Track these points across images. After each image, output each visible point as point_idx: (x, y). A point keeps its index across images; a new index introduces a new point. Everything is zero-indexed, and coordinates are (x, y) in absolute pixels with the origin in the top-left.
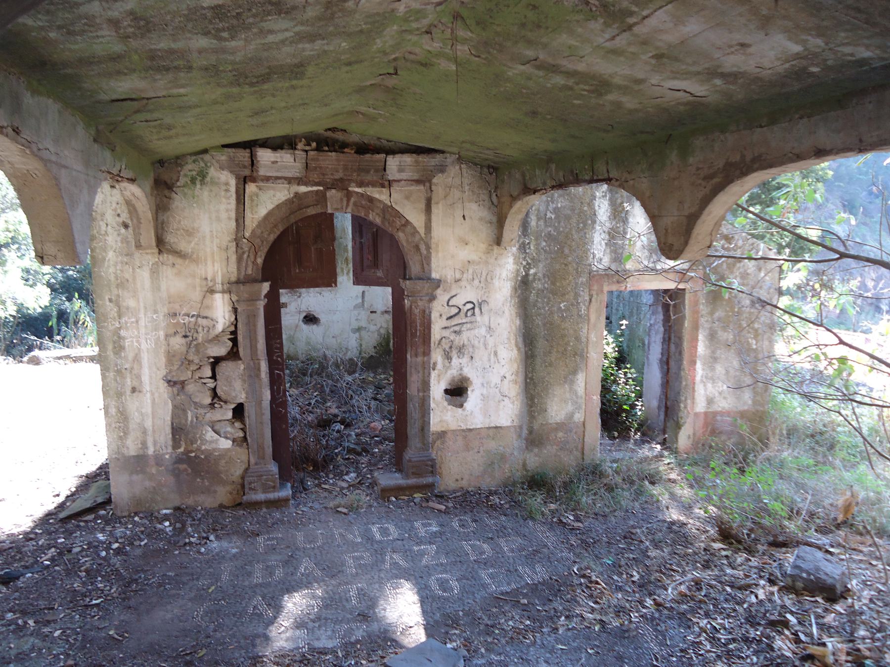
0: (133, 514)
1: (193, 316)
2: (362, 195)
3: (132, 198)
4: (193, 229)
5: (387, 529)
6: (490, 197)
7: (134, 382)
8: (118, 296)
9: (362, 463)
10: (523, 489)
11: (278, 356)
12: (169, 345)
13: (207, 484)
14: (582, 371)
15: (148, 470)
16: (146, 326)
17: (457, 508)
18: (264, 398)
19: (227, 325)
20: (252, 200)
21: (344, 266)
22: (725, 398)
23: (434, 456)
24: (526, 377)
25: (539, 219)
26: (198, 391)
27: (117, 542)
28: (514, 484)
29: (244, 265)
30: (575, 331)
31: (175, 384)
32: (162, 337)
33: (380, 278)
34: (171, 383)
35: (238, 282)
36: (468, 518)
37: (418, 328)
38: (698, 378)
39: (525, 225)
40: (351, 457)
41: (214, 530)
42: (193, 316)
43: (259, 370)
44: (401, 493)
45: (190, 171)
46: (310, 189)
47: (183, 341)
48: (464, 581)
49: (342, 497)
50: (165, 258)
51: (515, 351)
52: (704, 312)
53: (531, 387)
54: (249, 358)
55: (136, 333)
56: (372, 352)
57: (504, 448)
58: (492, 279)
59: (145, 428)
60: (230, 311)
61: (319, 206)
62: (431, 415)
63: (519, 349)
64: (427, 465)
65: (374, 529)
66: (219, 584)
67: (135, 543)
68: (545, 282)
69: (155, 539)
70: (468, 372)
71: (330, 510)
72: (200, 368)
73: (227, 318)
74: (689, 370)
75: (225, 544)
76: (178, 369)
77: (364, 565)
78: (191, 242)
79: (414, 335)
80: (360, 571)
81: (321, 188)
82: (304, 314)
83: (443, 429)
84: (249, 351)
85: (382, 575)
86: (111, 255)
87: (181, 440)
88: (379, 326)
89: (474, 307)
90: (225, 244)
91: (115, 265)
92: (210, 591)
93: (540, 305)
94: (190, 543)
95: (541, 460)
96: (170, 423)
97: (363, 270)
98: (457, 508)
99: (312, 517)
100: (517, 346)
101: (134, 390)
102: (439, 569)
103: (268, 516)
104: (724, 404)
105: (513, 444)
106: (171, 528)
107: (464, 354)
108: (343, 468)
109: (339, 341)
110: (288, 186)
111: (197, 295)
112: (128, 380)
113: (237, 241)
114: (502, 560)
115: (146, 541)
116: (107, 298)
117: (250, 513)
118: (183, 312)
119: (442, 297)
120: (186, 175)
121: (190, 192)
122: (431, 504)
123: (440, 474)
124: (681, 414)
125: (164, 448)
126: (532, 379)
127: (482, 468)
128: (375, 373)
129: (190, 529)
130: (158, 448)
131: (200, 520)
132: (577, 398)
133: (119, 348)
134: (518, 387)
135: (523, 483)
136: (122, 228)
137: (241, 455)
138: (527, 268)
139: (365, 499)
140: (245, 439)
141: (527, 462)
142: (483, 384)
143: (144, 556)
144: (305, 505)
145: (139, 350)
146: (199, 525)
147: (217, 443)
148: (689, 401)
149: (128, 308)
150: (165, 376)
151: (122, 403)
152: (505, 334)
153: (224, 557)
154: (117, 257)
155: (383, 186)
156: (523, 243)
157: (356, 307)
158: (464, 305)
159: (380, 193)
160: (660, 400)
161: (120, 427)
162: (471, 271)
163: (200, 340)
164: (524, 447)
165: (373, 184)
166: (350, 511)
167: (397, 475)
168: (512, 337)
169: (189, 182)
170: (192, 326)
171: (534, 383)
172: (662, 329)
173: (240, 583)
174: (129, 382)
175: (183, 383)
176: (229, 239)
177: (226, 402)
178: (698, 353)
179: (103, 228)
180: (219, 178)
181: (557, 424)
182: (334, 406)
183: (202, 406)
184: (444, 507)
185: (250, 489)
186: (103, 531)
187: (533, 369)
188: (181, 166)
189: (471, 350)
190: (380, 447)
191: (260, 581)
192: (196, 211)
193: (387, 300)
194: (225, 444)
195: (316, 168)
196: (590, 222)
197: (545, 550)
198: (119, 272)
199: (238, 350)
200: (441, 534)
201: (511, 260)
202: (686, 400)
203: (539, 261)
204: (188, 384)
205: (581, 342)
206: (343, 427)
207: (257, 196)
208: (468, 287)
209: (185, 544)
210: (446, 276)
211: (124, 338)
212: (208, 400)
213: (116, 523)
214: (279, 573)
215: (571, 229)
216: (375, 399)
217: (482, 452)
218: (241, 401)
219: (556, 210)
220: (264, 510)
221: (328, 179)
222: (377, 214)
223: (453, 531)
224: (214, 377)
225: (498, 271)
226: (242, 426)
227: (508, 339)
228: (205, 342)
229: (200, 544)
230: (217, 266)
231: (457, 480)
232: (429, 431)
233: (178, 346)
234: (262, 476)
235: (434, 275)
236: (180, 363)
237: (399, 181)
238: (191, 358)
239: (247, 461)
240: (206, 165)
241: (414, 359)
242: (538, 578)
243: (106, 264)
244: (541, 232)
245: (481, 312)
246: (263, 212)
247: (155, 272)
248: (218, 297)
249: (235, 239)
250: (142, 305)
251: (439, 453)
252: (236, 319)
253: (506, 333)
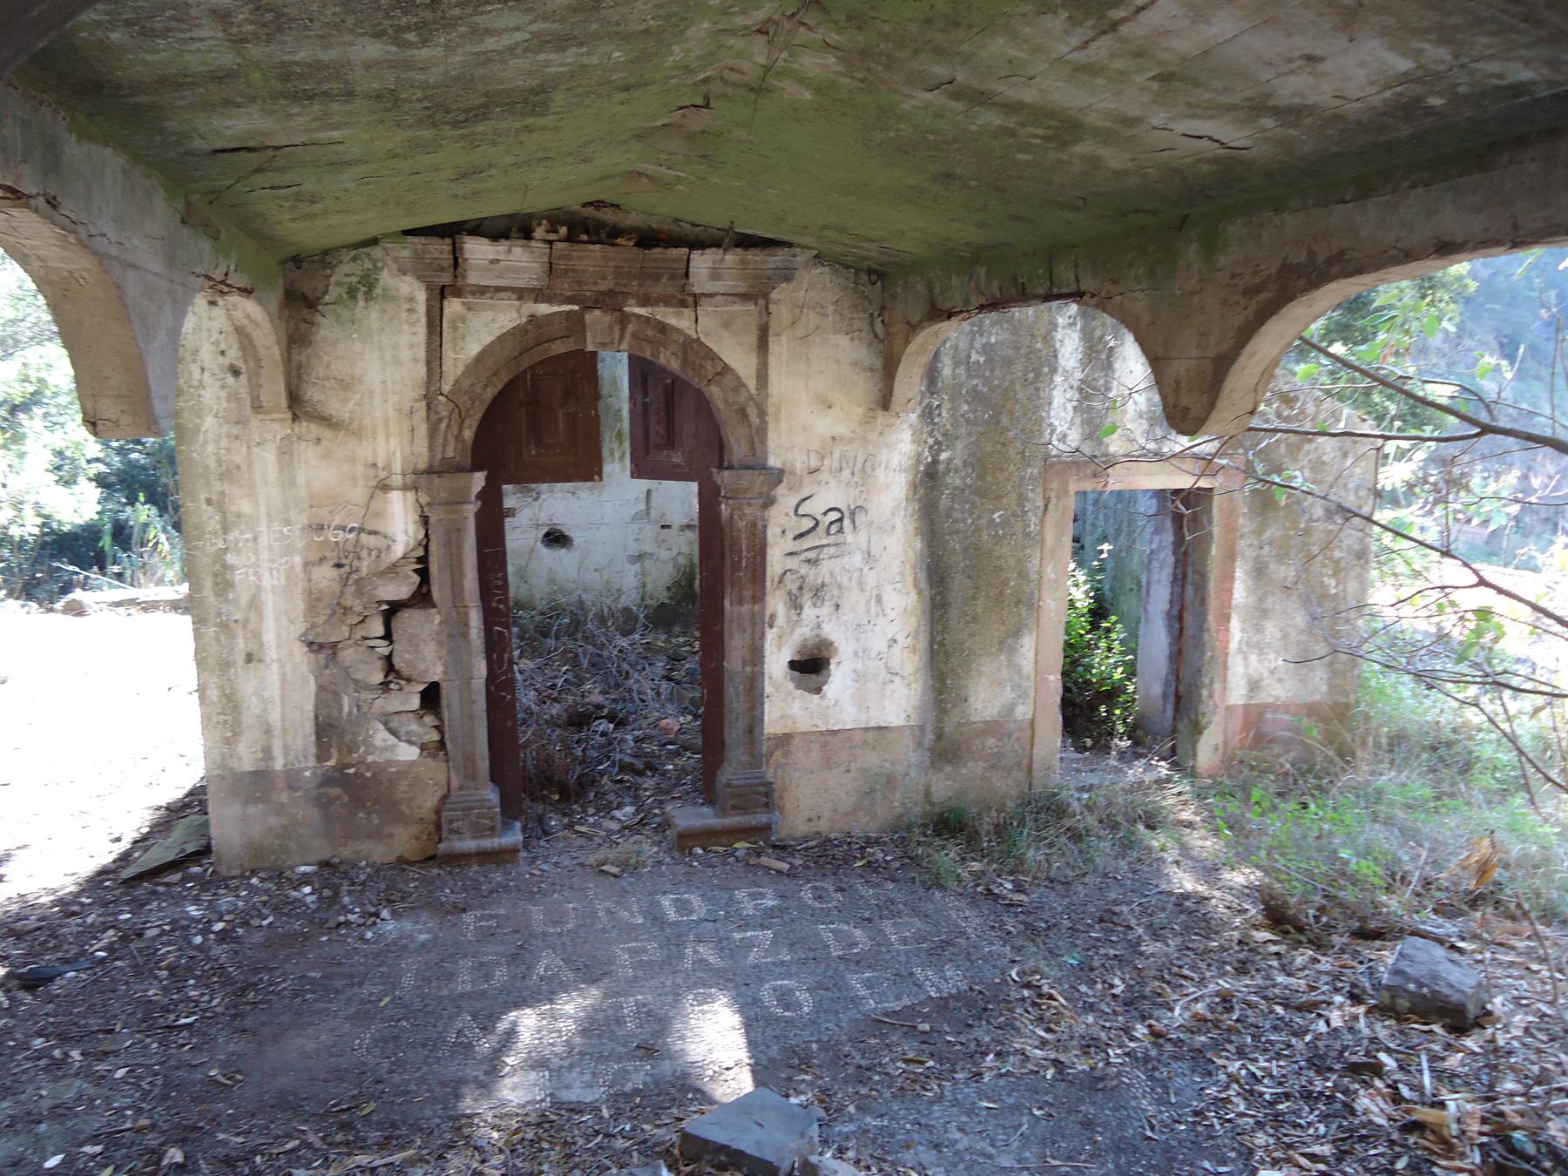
0: (247, 874)
1: (351, 530)
2: (648, 319)
3: (245, 322)
4: (352, 377)
5: (688, 901)
6: (872, 324)
7: (250, 646)
8: (222, 493)
9: (646, 789)
10: (925, 835)
11: (499, 601)
12: (310, 581)
13: (376, 821)
14: (1031, 631)
15: (275, 797)
16: (270, 548)
17: (809, 868)
18: (475, 673)
19: (411, 546)
20: (455, 328)
21: (615, 446)
22: (1280, 680)
23: (769, 776)
24: (932, 641)
25: (956, 364)
26: (362, 661)
27: (220, 920)
28: (909, 828)
29: (441, 441)
30: (1019, 561)
32: (298, 565)
33: (678, 466)
34: (314, 646)
35: (430, 471)
36: (828, 885)
37: (744, 554)
38: (1233, 645)
39: (932, 374)
40: (626, 778)
41: (389, 901)
42: (351, 530)
43: (466, 624)
44: (713, 840)
45: (346, 275)
46: (556, 309)
47: (335, 573)
48: (821, 992)
49: (611, 847)
50: (304, 429)
51: (914, 596)
52: (1245, 530)
53: (941, 657)
54: (449, 604)
55: (253, 559)
56: (663, 597)
57: (892, 764)
58: (874, 469)
59: (268, 724)
60: (415, 522)
61: (571, 340)
62: (766, 706)
63: (920, 592)
64: (758, 794)
65: (666, 902)
66: (397, 993)
67: (252, 922)
68: (967, 476)
69: (286, 915)
70: (831, 631)
71: (589, 870)
72: (362, 621)
73: (411, 533)
74: (1218, 631)
75: (407, 926)
76: (326, 621)
77: (649, 963)
78: (346, 401)
79: (736, 567)
80: (640, 973)
81: (576, 308)
83: (787, 731)
84: (448, 593)
85: (679, 980)
86: (209, 422)
87: (331, 746)
88: (675, 551)
89: (841, 519)
90: (407, 404)
91: (218, 440)
92: (382, 1004)
93: (957, 515)
94: (347, 924)
95: (957, 786)
96: (312, 715)
97: (648, 453)
98: (809, 868)
99: (557, 881)
100: (916, 586)
101: (250, 658)
102: (778, 970)
103: (482, 879)
104: (1278, 691)
105: (908, 758)
106: (314, 898)
107: (823, 600)
108: (611, 797)
109: (605, 577)
110: (516, 303)
111: (358, 494)
112: (240, 640)
113: (429, 398)
114: (888, 957)
115: (271, 919)
116: (203, 496)
117: (450, 873)
118: (335, 523)
119: (786, 500)
120: (339, 284)
121: (346, 313)
122: (764, 860)
123: (781, 809)
124: (1202, 708)
125: (301, 759)
126: (942, 644)
127: (853, 799)
128: (669, 633)
129: (346, 900)
130: (290, 758)
131: (363, 883)
132: (1021, 678)
133: (224, 585)
134: (917, 658)
135: (925, 826)
136: (229, 375)
137: (435, 772)
138: (936, 449)
139: (649, 850)
140: (441, 744)
141: (933, 789)
142: (856, 653)
143: (267, 944)
144: (546, 860)
145: (259, 588)
146: (362, 892)
147: (393, 751)
148: (1217, 686)
149: (239, 516)
150: (304, 635)
152: (896, 567)
153: (405, 947)
154: (221, 426)
155: (684, 304)
156: (929, 406)
157: (635, 518)
158: (825, 514)
159: (679, 315)
160: (1167, 684)
161: (226, 721)
162: (836, 455)
163: (364, 571)
164: (928, 762)
165: (666, 301)
166: (623, 871)
167: (705, 809)
168: (909, 572)
169: (345, 296)
170: (349, 547)
171: (946, 652)
172: (1171, 559)
173: (434, 991)
174: (241, 645)
175: (334, 645)
176: (414, 395)
177: (409, 680)
178: (1234, 602)
179: (196, 375)
180: (397, 290)
181: (985, 722)
182: (597, 690)
183: (368, 688)
184: (788, 866)
185: (451, 831)
186: (196, 901)
187: (945, 628)
188: (331, 266)
189: (835, 592)
190: (677, 761)
191: (469, 987)
192: (357, 346)
193: (690, 506)
194: (408, 753)
195: (566, 272)
196: (1046, 370)
197: (962, 941)
198: (223, 451)
199: (429, 591)
200: (782, 910)
201: (907, 436)
202: (1211, 683)
203: (957, 438)
204: (343, 649)
205: (1029, 581)
206: (612, 726)
207: (464, 320)
208: (832, 483)
209: (339, 925)
210: (793, 465)
211: (232, 568)
212: (378, 677)
213: (219, 888)
214: (501, 975)
215: (1013, 382)
216: (669, 679)
217: (853, 773)
218: (436, 679)
219: (987, 349)
220: (476, 868)
221: (588, 290)
222: (673, 354)
223: (803, 907)
224: (388, 636)
225: (884, 455)
226: (437, 722)
227: (902, 574)
228: (374, 575)
229: (364, 924)
230: (394, 442)
231: (810, 820)
232: (762, 733)
233: (325, 583)
234: (471, 809)
235: (773, 462)
236: (329, 612)
237: (711, 295)
238: (348, 603)
239: (444, 783)
240: (375, 266)
241: (736, 608)
242: (949, 988)
243: (201, 437)
244: (961, 386)
245: (855, 527)
246: (473, 348)
247: (285, 453)
248: (395, 496)
249: (426, 396)
250: (263, 510)
251: (780, 772)
252: (427, 535)
253: (898, 563)
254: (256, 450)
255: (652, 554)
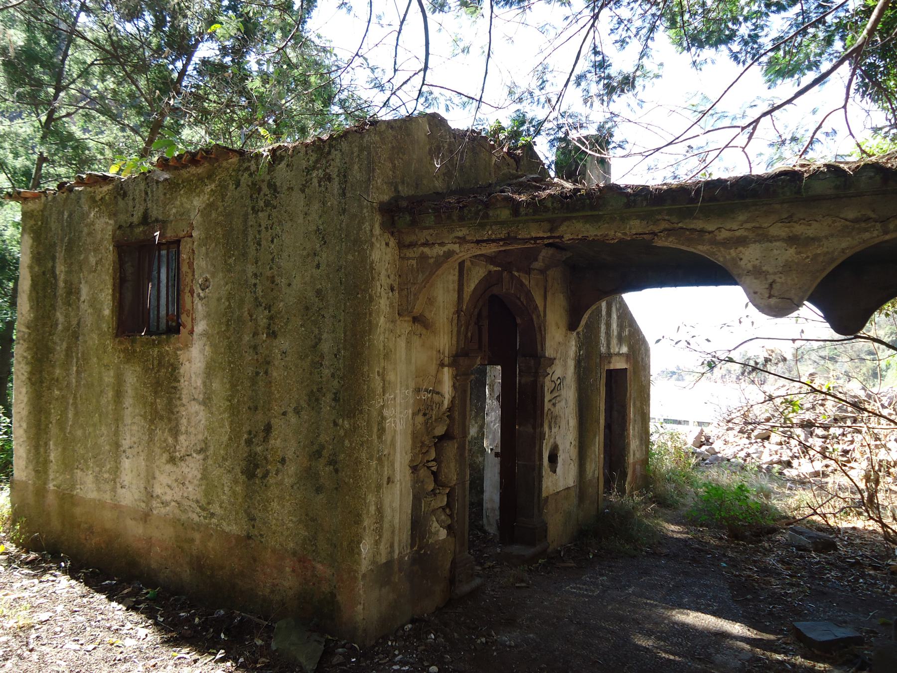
0: (381, 641)
31: (414, 469)
32: (410, 416)
86: (382, 319)
112: (386, 469)
113: (458, 312)
145: (395, 431)
151: (380, 498)
246: (473, 286)
248: (446, 369)
254: (398, 339)
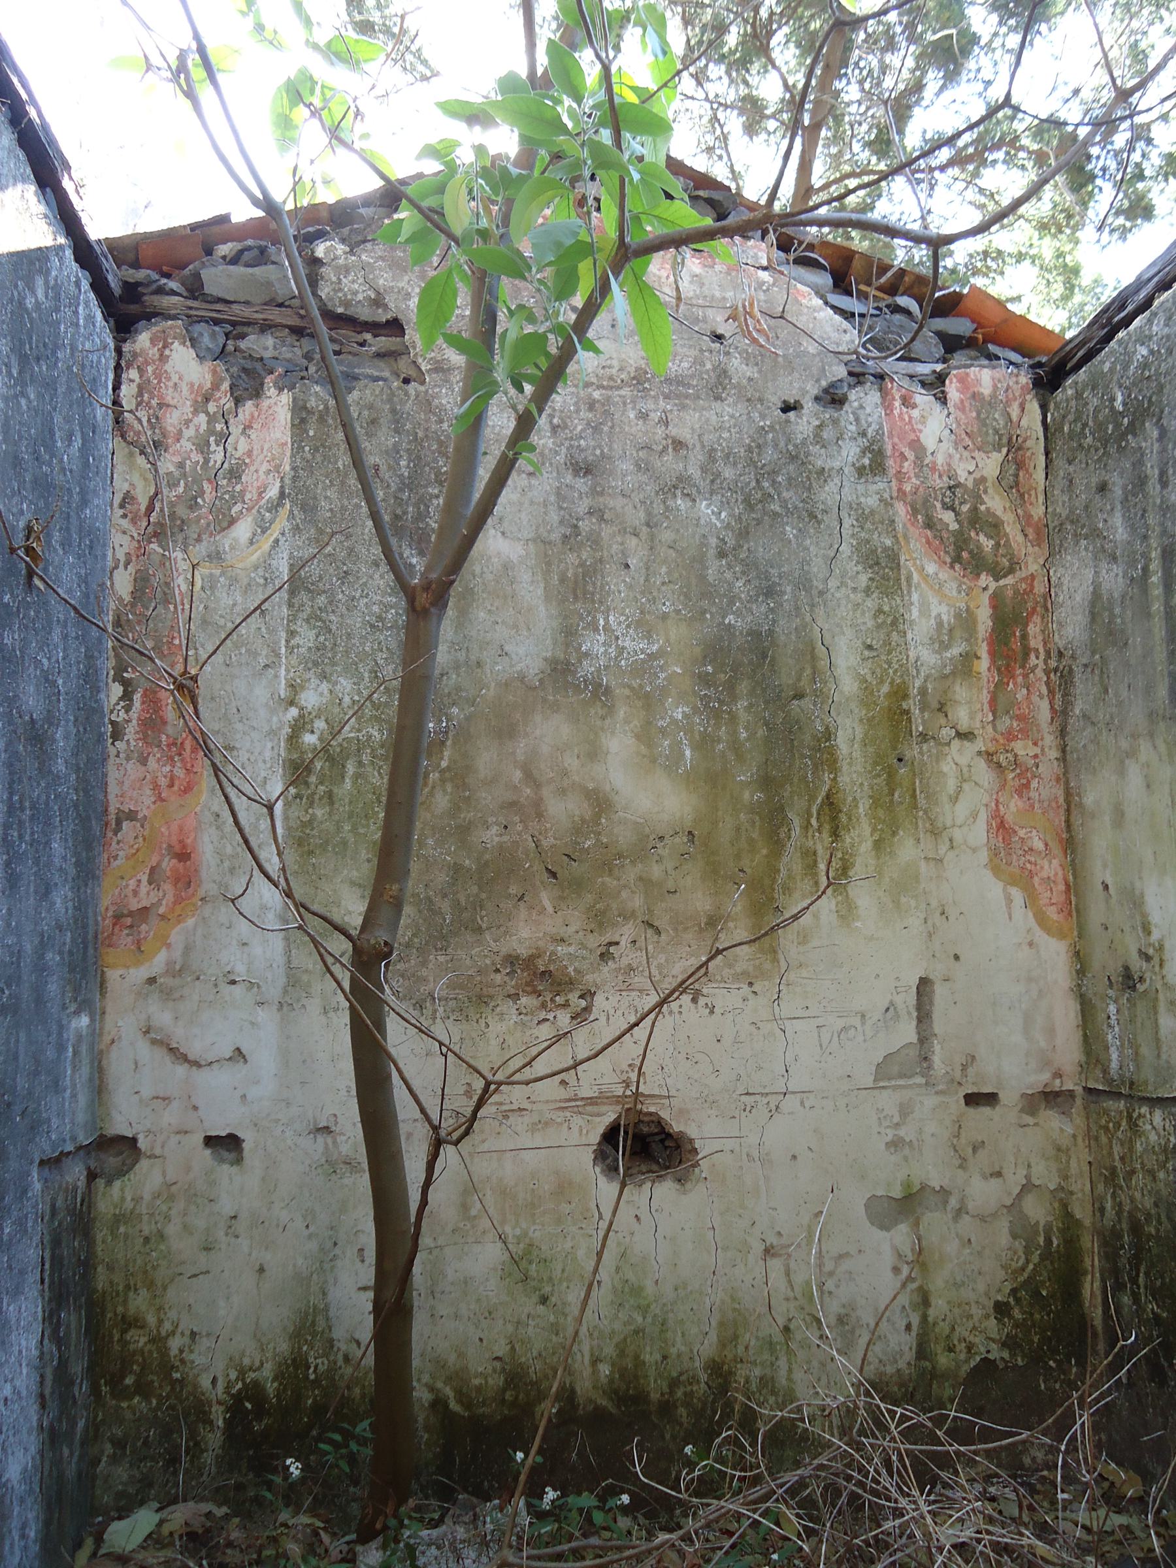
21: (821, 843)
82: (609, 1116)
88: (1015, 1180)
157: (885, 1071)
193: (1051, 1032)
255: (944, 1193)
